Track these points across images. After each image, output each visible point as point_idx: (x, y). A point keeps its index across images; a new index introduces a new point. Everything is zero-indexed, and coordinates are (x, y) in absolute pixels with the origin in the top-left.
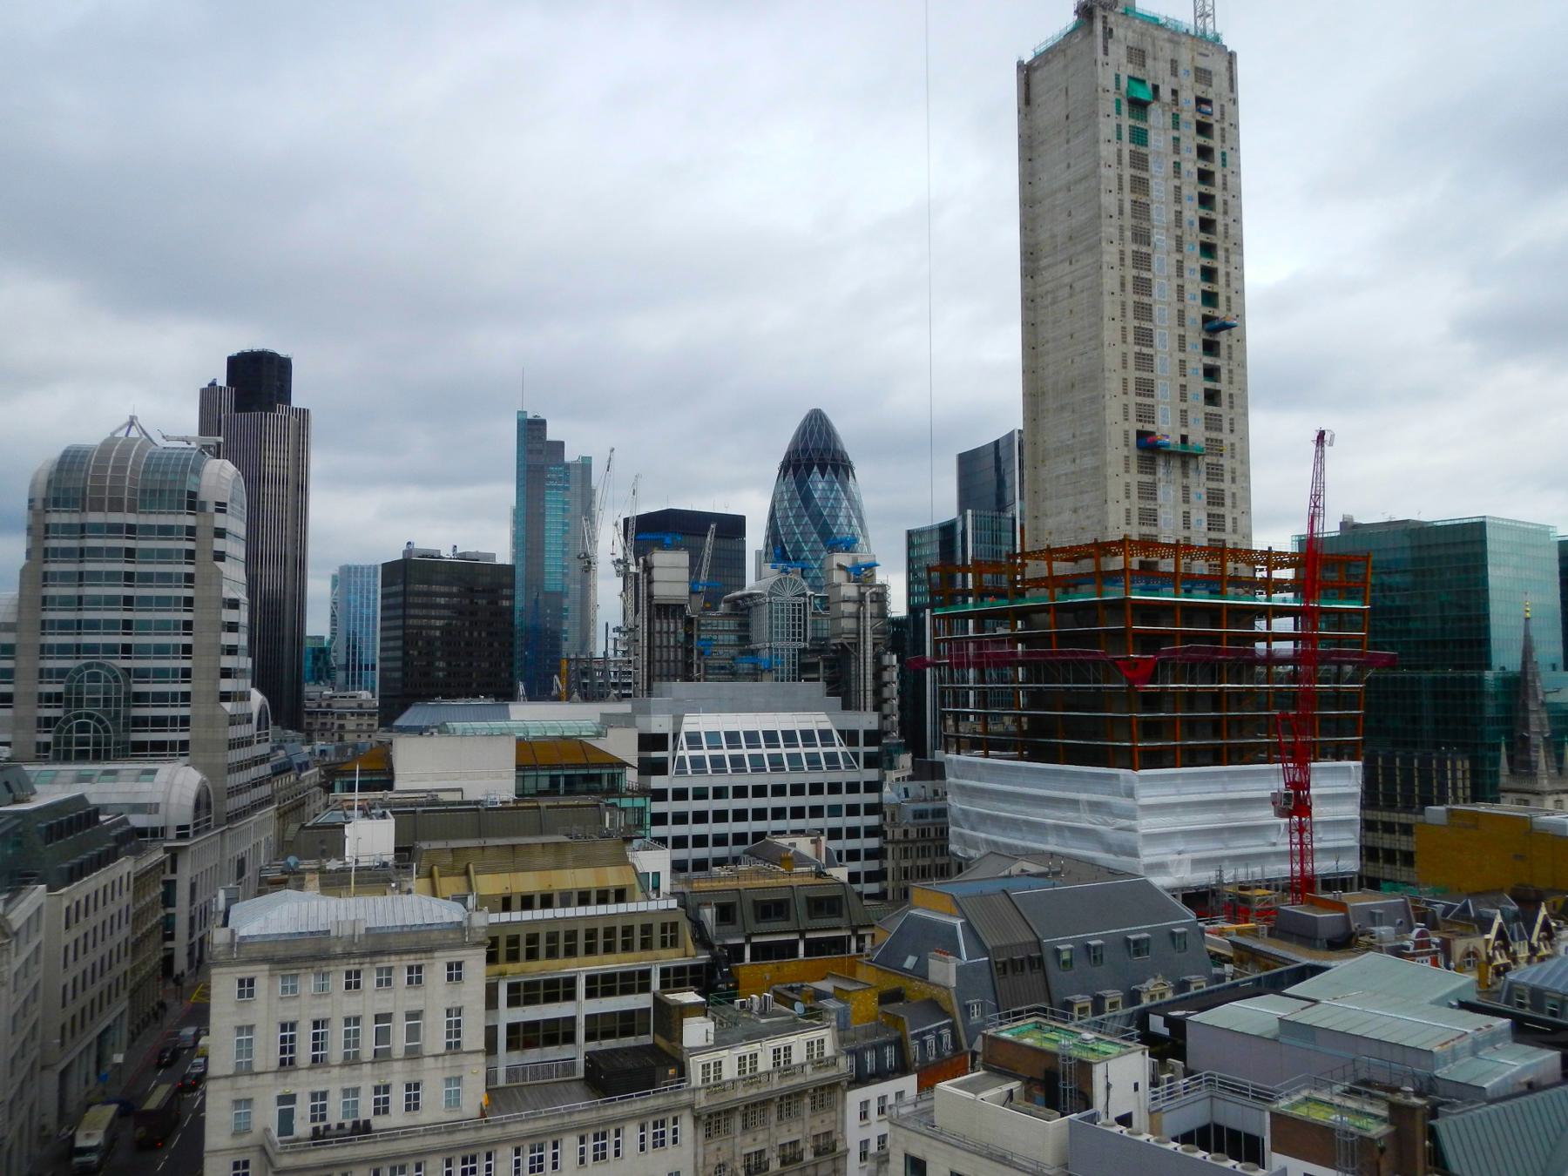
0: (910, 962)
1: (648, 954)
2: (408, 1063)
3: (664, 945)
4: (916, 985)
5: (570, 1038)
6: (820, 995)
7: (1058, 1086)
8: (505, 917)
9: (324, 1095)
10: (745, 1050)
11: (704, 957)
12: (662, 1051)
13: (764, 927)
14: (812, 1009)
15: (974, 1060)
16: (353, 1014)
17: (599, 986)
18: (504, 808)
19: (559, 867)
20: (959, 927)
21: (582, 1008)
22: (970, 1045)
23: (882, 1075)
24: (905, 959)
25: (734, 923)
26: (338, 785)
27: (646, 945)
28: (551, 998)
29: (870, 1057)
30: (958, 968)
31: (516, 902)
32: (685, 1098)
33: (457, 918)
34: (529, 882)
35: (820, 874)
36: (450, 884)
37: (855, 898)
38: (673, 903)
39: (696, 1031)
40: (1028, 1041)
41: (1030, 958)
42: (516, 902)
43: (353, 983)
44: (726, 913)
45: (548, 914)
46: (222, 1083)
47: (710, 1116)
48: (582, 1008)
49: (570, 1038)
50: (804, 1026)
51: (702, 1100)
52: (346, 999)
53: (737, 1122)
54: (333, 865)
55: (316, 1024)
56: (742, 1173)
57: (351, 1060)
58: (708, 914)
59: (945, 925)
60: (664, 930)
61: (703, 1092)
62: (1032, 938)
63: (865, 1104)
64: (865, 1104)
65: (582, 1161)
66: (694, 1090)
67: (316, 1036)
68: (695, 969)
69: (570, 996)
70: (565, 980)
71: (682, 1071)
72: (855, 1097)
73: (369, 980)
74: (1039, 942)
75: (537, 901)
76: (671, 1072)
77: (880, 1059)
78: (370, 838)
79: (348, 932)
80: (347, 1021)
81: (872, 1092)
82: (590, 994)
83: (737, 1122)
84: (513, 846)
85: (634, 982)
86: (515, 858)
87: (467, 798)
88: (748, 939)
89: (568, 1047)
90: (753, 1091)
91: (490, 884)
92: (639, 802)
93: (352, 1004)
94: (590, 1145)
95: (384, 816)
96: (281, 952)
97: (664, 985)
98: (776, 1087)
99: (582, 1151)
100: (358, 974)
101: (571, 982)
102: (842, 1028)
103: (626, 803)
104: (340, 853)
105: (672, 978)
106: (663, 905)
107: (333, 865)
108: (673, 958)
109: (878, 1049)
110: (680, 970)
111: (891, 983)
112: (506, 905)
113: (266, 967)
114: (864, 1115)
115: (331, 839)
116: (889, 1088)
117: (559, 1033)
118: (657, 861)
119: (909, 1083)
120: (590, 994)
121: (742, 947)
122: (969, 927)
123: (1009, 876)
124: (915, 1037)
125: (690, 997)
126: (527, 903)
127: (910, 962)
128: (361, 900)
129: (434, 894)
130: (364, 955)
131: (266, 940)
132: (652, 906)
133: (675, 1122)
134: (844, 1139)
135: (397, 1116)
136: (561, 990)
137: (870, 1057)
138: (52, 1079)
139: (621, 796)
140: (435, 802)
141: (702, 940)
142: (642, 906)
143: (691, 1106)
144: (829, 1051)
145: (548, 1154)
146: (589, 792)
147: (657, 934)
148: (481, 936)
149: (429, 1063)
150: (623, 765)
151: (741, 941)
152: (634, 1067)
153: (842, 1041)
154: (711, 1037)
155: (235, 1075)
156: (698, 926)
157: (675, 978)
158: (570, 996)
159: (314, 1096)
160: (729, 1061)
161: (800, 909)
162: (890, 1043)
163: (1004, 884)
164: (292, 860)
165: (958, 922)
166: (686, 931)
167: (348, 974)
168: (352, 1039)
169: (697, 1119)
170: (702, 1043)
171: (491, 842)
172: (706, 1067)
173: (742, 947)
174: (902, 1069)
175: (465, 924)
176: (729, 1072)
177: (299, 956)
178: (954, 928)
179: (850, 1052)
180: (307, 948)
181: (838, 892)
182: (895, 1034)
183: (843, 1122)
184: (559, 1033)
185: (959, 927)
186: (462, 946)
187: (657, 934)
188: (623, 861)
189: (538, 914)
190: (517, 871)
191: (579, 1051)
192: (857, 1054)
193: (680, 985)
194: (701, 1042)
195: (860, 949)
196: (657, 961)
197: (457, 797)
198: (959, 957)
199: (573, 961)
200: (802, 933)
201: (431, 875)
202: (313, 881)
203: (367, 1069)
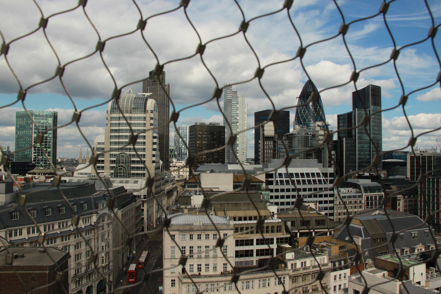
0: (347, 239)
1: (273, 234)
2: (214, 259)
3: (277, 232)
4: (349, 244)
5: (252, 255)
6: (323, 246)
7: (399, 273)
8: (235, 222)
9: (200, 265)
10: (303, 260)
11: (289, 236)
12: (280, 260)
13: (303, 227)
14: (321, 250)
15: (366, 266)
16: (192, 246)
17: (260, 242)
18: (231, 194)
19: (249, 210)
20: (362, 229)
21: (255, 247)
22: (365, 261)
23: (341, 269)
24: (346, 238)
25: (295, 226)
26: (186, 186)
27: (272, 231)
28: (247, 244)
29: (337, 264)
30: (362, 240)
31: (237, 219)
32: (287, 272)
33: (226, 222)
34: (241, 213)
35: (319, 214)
36: (221, 213)
37: (329, 220)
38: (280, 220)
39: (289, 256)
40: (389, 260)
41: (382, 238)
42: (237, 219)
43: (199, 237)
44: (293, 224)
45: (246, 222)
46: (168, 260)
47: (293, 277)
48: (255, 247)
49: (252, 255)
50: (319, 255)
51: (291, 273)
52: (198, 242)
53: (300, 279)
54: (189, 207)
55: (190, 247)
56: (302, 292)
57: (199, 257)
58: (289, 224)
59: (358, 228)
60: (277, 227)
61: (292, 271)
62: (383, 232)
63: (335, 276)
64: (335, 276)
65: (259, 286)
66: (289, 270)
67: (190, 250)
68: (286, 238)
69: (252, 244)
70: (251, 240)
71: (286, 266)
72: (333, 274)
73: (203, 237)
74: (385, 233)
75: (248, 218)
76: (283, 265)
77: (340, 264)
78: (197, 200)
79: (198, 224)
80: (198, 247)
81: (337, 273)
82: (257, 244)
83: (300, 279)
84: (236, 204)
85: (270, 241)
86: (236, 206)
87: (220, 190)
88: (299, 231)
89: (252, 257)
90: (305, 271)
91: (231, 213)
92: (267, 192)
93: (199, 243)
94: (261, 283)
95: (200, 194)
96: (181, 228)
97: (277, 242)
98: (311, 270)
99: (260, 284)
100: (200, 235)
101: (252, 240)
102: (329, 255)
103: (263, 192)
104: (190, 204)
105: (279, 241)
106: (277, 221)
107: (189, 207)
108: (280, 235)
109: (340, 262)
110: (282, 239)
111: (343, 244)
112: (235, 219)
113: (178, 232)
114: (335, 279)
115: (187, 200)
116: (342, 272)
117: (249, 253)
118: (273, 209)
119: (348, 271)
120: (257, 244)
121: (296, 233)
122: (365, 229)
123: (375, 215)
124: (349, 259)
125: (287, 246)
126: (240, 219)
127: (347, 239)
128: (200, 216)
129: (216, 215)
130: (202, 230)
131: (180, 225)
132: (274, 221)
133: (284, 278)
134: (330, 285)
135: (211, 272)
136: (250, 243)
137: (337, 264)
138: (120, 256)
139: (262, 191)
140: (212, 191)
141: (288, 231)
142: (272, 221)
143: (288, 274)
144: (326, 261)
145: (251, 284)
146: (255, 190)
147: (275, 229)
148: (232, 227)
149: (219, 259)
150: (262, 182)
151: (297, 231)
152: (271, 264)
153: (329, 259)
154: (294, 256)
155: (171, 258)
156: (286, 227)
157: (280, 241)
158: (252, 244)
159: (198, 265)
160: (299, 263)
161: (313, 223)
162: (343, 260)
163: (375, 217)
164: (179, 205)
165: (362, 227)
166: (283, 228)
167: (198, 235)
168: (200, 252)
169: (290, 277)
170: (291, 258)
171: (230, 202)
172: (292, 264)
173: (296, 233)
174: (346, 267)
175: (228, 224)
176: (299, 266)
177: (188, 230)
178: (360, 229)
179: (332, 262)
180: (188, 228)
181: (324, 218)
182: (343, 258)
183: (329, 281)
184: (249, 253)
185: (362, 229)
186: (227, 229)
187: (275, 229)
188: (266, 208)
189: (243, 222)
190: (237, 210)
191: (255, 259)
192: (334, 263)
193: (282, 242)
194: (291, 258)
195: (330, 234)
196: (275, 236)
197: (217, 190)
198: (362, 237)
199: (253, 235)
200: (314, 231)
201: (224, 210)
202: (186, 211)
203: (203, 259)
